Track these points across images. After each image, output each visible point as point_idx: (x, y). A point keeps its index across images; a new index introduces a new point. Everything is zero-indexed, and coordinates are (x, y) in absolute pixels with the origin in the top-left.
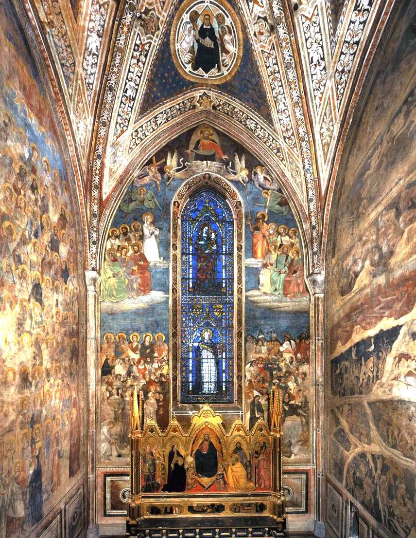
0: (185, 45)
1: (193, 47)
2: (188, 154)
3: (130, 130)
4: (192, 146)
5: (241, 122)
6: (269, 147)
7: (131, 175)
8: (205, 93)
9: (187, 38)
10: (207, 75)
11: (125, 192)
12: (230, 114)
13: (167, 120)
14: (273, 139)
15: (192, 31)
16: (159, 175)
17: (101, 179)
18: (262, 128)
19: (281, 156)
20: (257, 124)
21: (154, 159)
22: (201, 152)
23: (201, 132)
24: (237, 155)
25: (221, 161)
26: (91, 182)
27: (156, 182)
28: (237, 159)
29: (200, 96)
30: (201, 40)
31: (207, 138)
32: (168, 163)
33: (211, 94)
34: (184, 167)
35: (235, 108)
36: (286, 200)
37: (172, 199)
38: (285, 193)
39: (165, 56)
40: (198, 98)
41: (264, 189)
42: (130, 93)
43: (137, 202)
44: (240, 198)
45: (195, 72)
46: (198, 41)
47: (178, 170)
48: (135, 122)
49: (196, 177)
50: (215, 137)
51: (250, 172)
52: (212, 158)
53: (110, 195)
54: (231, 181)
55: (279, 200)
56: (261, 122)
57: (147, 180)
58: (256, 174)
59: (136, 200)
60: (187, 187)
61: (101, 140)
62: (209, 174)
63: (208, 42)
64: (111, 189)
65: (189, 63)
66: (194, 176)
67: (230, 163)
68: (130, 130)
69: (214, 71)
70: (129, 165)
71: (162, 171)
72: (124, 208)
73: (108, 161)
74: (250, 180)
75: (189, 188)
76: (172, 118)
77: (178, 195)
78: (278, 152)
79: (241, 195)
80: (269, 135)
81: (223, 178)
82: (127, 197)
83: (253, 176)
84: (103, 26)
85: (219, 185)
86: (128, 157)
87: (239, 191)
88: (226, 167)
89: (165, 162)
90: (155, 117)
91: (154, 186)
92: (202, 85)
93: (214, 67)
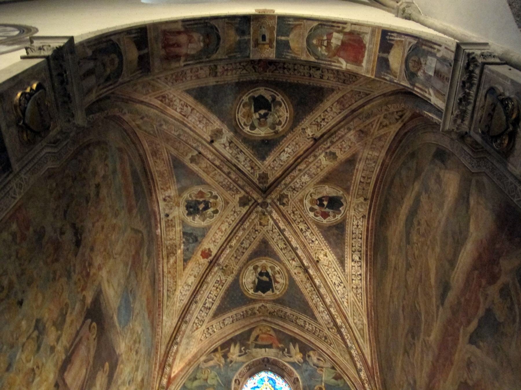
0: (249, 280)
1: (255, 281)
2: (249, 345)
3: (204, 327)
4: (252, 338)
5: (292, 322)
6: (318, 336)
7: (198, 359)
8: (263, 305)
9: (251, 277)
10: (266, 294)
11: (191, 372)
12: (283, 317)
13: (233, 322)
14: (320, 330)
15: (254, 274)
16: (223, 360)
17: (174, 359)
18: (309, 324)
19: (329, 342)
20: (305, 322)
21: (219, 349)
22: (260, 342)
23: (260, 330)
24: (291, 344)
25: (278, 348)
26: (166, 361)
27: (219, 365)
28: (291, 347)
29: (260, 307)
30: (260, 278)
31: (265, 333)
32: (231, 351)
33: (268, 305)
34: (246, 353)
35: (286, 313)
36: (340, 375)
37: (233, 377)
38: (338, 370)
39: (236, 285)
40: (258, 308)
41: (318, 367)
42: (207, 305)
43: (202, 380)
44: (297, 374)
45: (256, 293)
46: (258, 278)
47: (240, 356)
48: (208, 322)
49: (256, 361)
50: (272, 333)
51: (304, 355)
52: (270, 346)
53: (178, 374)
54: (288, 362)
55: (334, 375)
56: (308, 320)
57: (211, 363)
58: (309, 356)
59: (200, 379)
60: (248, 368)
61: (181, 333)
62: (267, 358)
63: (265, 278)
64: (179, 369)
65: (252, 288)
66: (254, 360)
67: (286, 350)
68: (204, 327)
69: (269, 292)
70: (198, 352)
71: (225, 356)
72: (189, 385)
73: (181, 349)
74: (305, 361)
75: (249, 369)
76: (237, 320)
77: (240, 374)
78: (326, 338)
79: (298, 373)
80: (316, 328)
81: (281, 360)
82: (192, 377)
83: (307, 358)
84: (198, 273)
85: (277, 366)
86: (197, 346)
87: (296, 369)
88: (283, 352)
89: (229, 351)
90: (224, 320)
91: (218, 367)
92: (261, 300)
93: (268, 290)
